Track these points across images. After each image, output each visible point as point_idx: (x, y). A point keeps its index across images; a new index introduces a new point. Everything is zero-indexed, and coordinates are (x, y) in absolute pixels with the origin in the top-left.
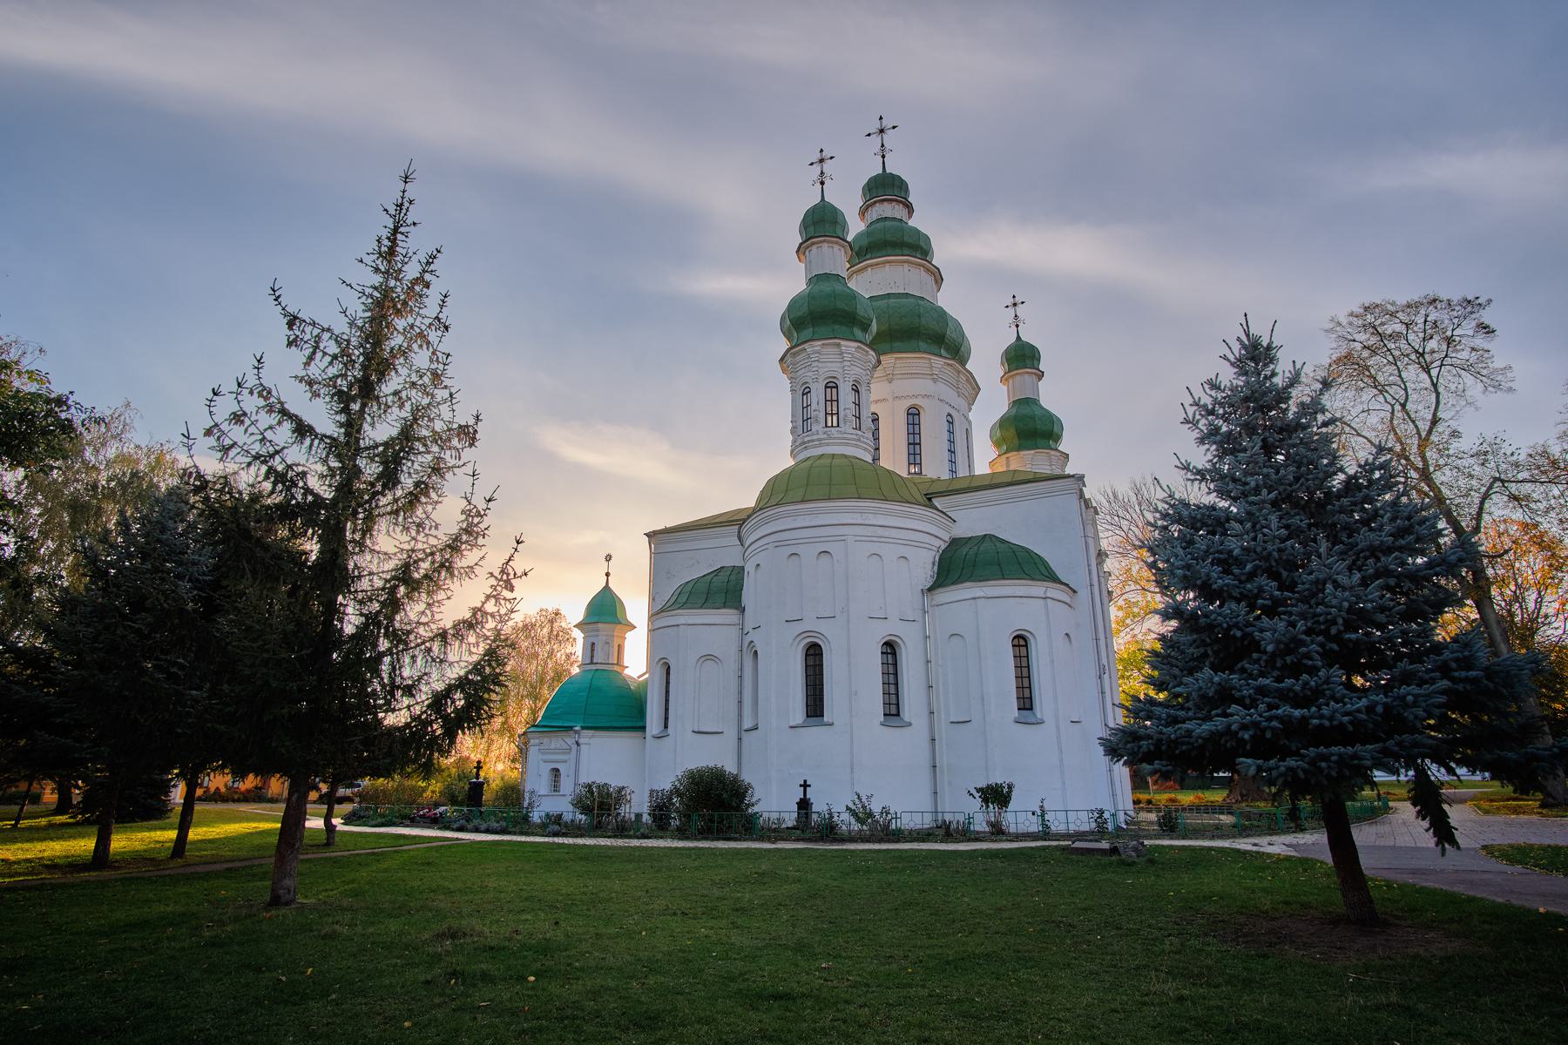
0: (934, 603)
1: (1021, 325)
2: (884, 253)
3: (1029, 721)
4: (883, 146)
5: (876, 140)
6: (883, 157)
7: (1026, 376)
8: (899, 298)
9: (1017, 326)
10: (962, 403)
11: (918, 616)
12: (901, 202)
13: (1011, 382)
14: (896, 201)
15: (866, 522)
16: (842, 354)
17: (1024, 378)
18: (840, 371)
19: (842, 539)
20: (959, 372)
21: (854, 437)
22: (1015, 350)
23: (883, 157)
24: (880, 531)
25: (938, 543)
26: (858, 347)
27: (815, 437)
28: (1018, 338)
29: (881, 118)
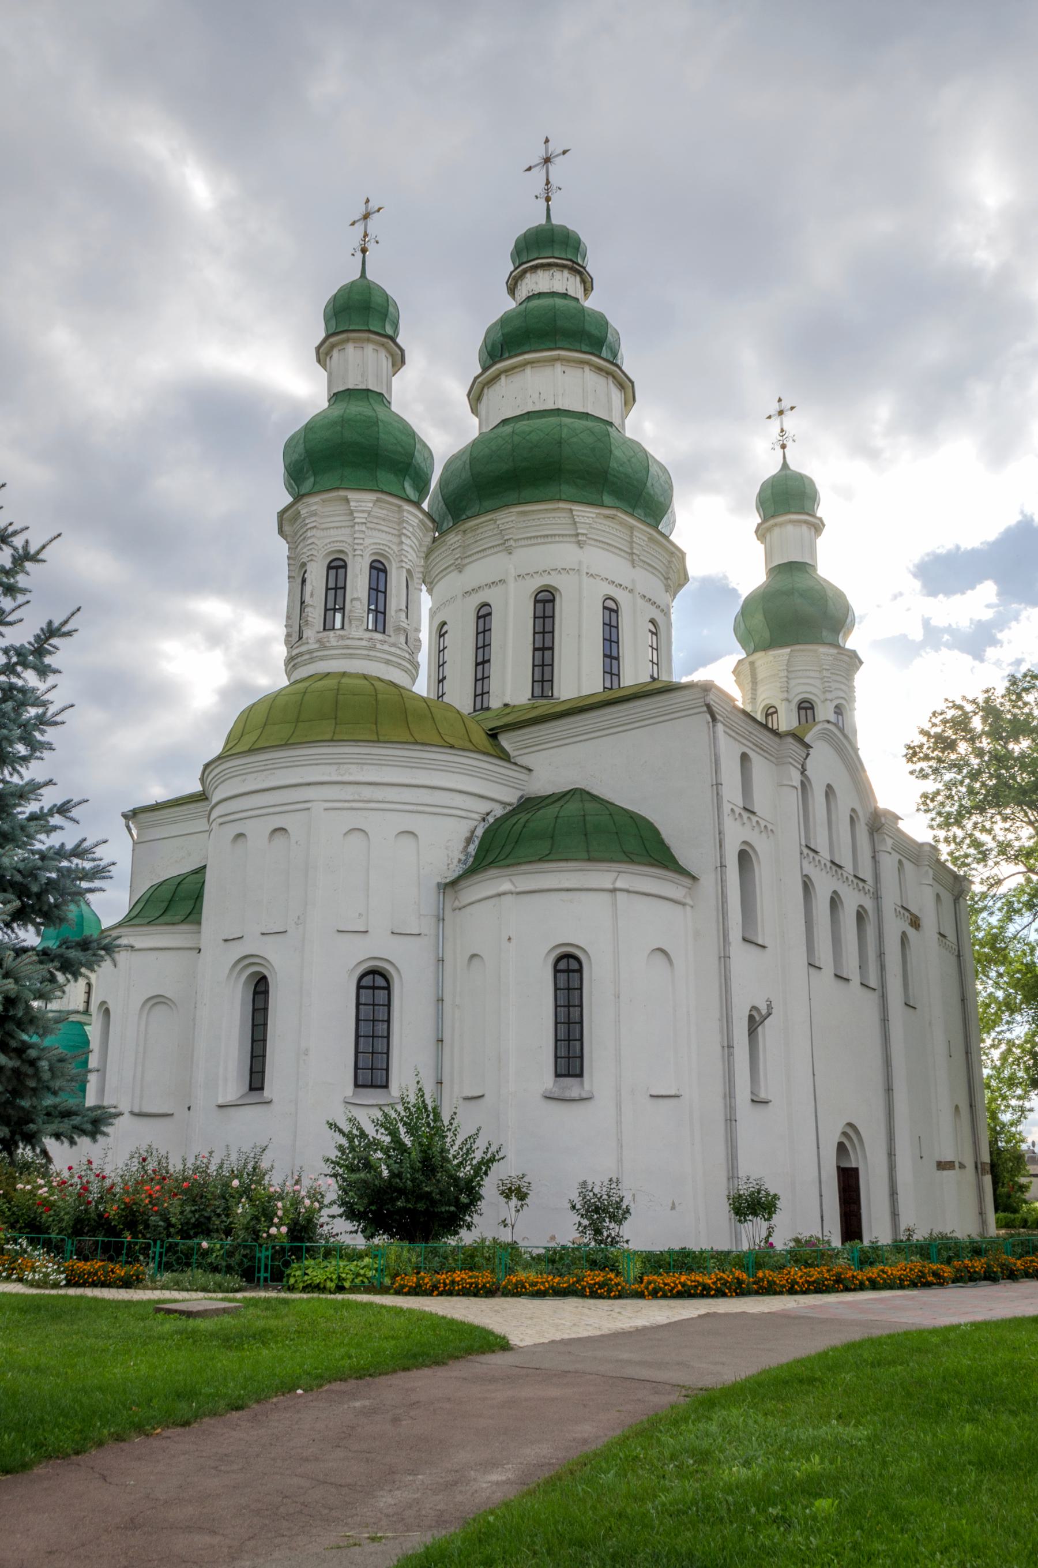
0: (457, 904)
1: (789, 444)
2: (526, 348)
3: (568, 1094)
4: (548, 183)
5: (539, 174)
6: (548, 199)
7: (790, 528)
8: (544, 417)
9: (783, 447)
10: (649, 583)
11: (427, 926)
12: (564, 266)
13: (768, 537)
14: (557, 265)
15: (346, 778)
16: (351, 513)
17: (789, 530)
18: (350, 540)
19: (304, 807)
20: (632, 528)
21: (364, 643)
22: (773, 486)
23: (548, 199)
24: (367, 792)
25: (484, 807)
26: (378, 500)
27: (303, 649)
28: (785, 465)
29: (547, 141)
